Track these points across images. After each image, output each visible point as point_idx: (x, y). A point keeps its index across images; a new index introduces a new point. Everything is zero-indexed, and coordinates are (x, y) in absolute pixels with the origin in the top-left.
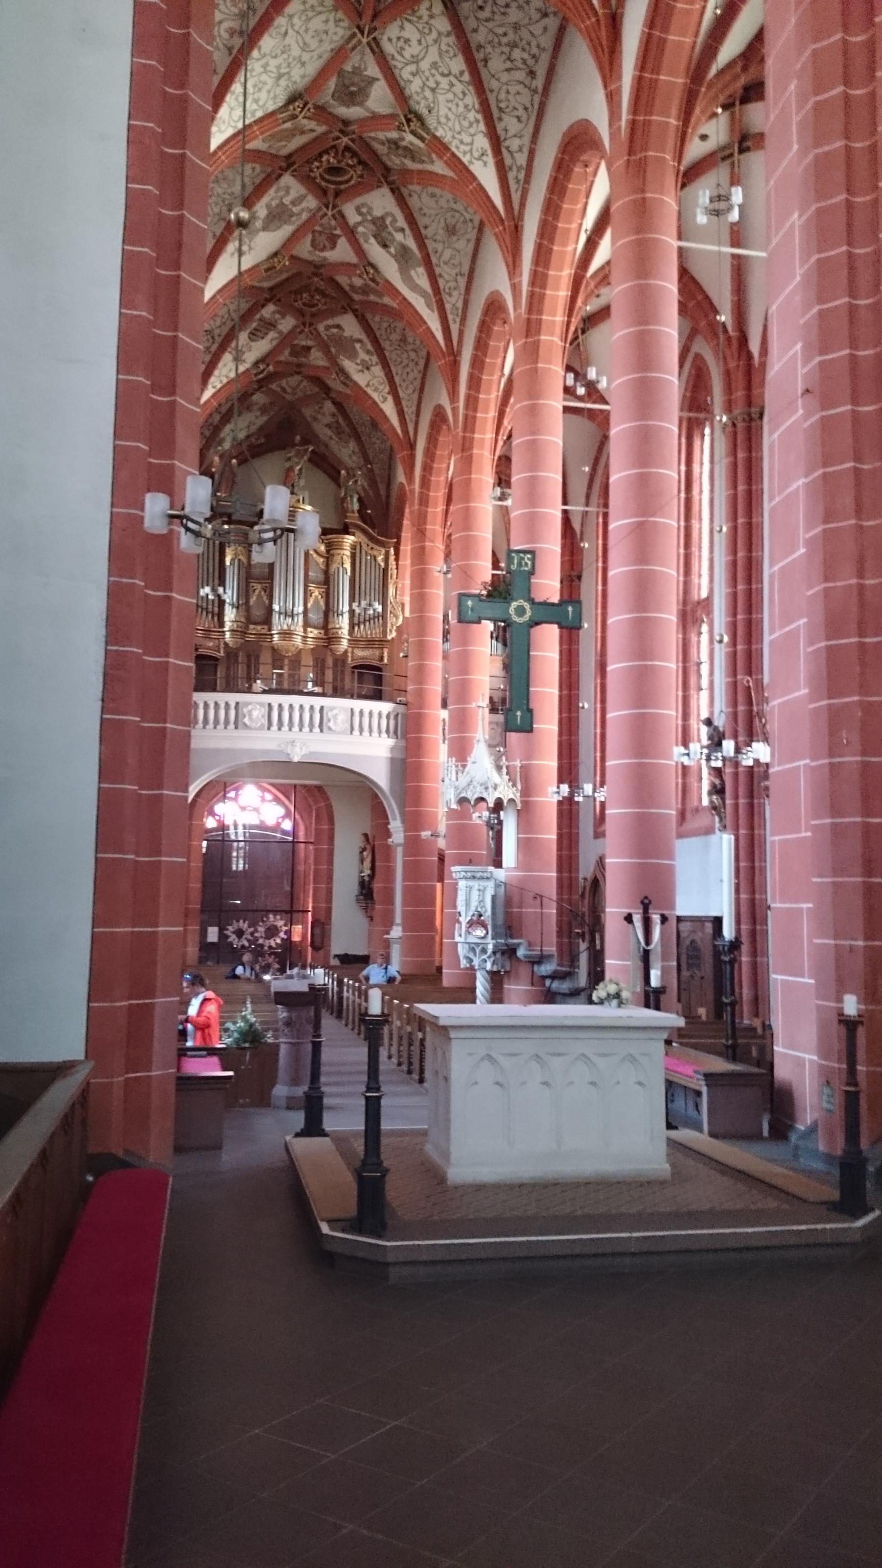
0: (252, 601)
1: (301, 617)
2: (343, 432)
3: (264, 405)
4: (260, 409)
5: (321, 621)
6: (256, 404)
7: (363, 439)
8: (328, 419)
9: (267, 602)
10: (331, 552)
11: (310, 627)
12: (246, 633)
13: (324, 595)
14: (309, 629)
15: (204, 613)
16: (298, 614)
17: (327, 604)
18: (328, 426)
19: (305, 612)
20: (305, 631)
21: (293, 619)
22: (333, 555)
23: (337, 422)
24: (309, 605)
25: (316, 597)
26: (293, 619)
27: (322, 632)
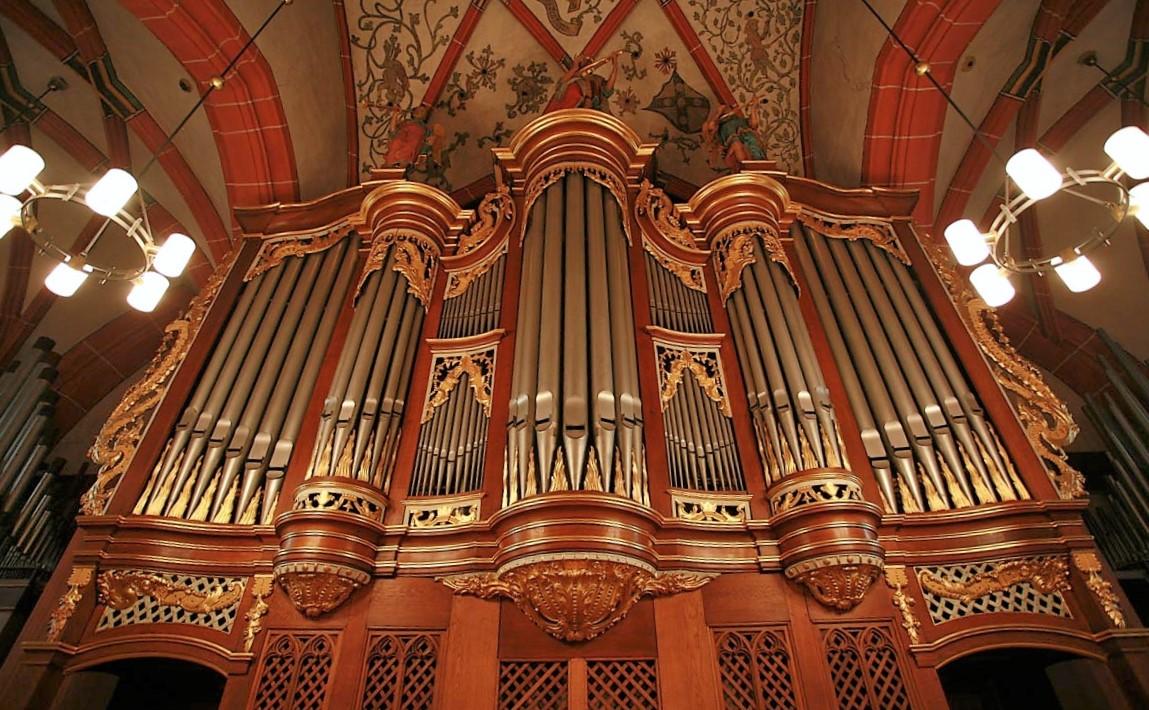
0: (435, 398)
1: (631, 436)
2: (690, 102)
3: (518, 69)
4: (512, 83)
5: (726, 458)
6: (501, 63)
7: (736, 95)
8: (658, 79)
9: (487, 402)
10: (718, 238)
11: (681, 483)
12: (381, 538)
13: (719, 364)
14: (679, 497)
15: (232, 464)
16: (617, 424)
17: (739, 383)
18: (656, 105)
19: (651, 421)
20: (660, 501)
21: (591, 442)
22: (727, 243)
23: (677, 78)
24: (665, 398)
25: (688, 375)
26: (591, 442)
27: (742, 502)
